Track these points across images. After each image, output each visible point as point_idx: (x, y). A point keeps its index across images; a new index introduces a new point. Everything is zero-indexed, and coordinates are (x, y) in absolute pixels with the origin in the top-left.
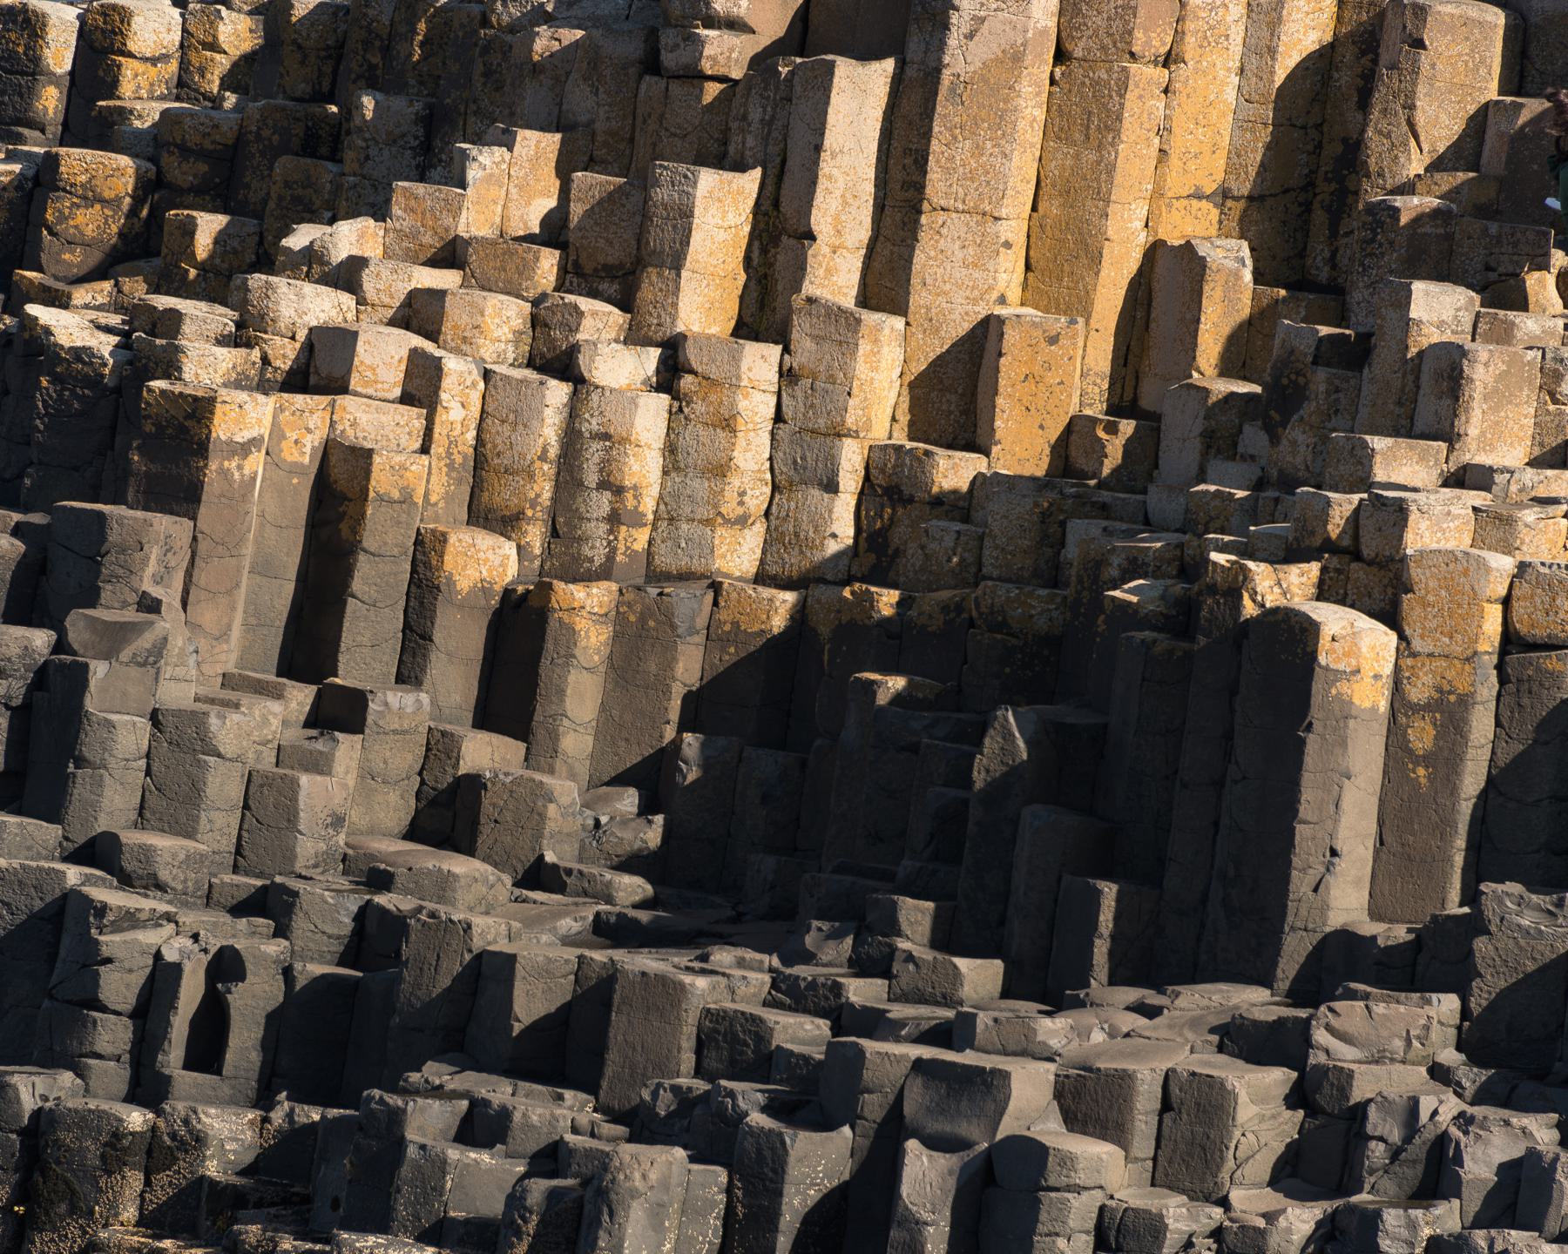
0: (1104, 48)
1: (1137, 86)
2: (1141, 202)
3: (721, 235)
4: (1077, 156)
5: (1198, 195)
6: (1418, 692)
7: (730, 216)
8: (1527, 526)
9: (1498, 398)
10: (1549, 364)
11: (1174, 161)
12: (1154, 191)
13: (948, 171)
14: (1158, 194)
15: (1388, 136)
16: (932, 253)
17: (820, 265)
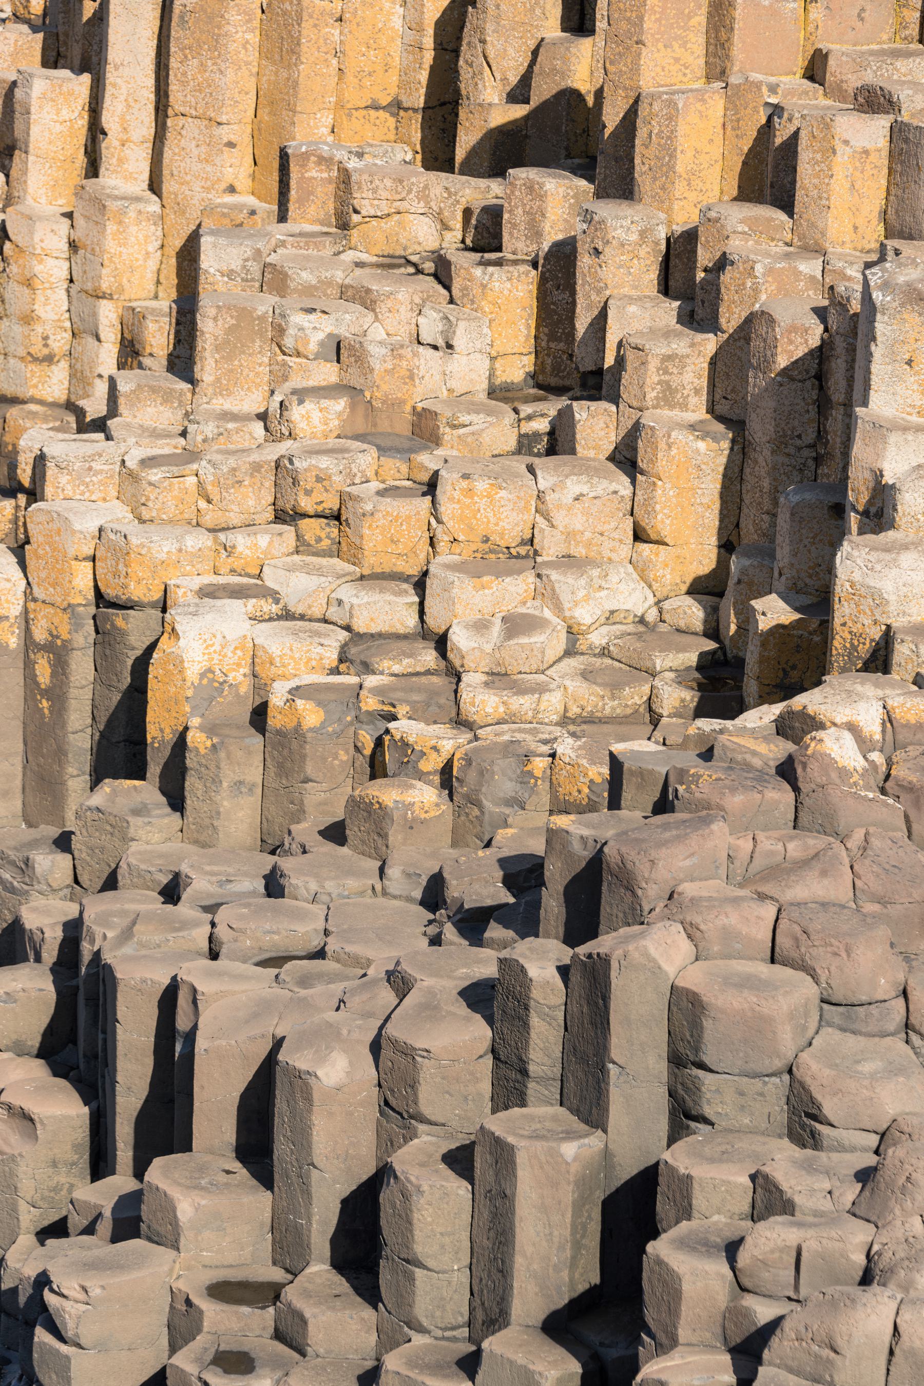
1: (311, 17)
2: (326, 113)
3: (58, 128)
4: (276, 74)
5: (377, 108)
6: (40, 635)
7: (64, 112)
8: (150, 484)
10: (279, 320)
11: (349, 77)
12: (336, 103)
13: (184, 84)
14: (340, 105)
15: (471, 66)
16: (177, 150)
17: (113, 155)
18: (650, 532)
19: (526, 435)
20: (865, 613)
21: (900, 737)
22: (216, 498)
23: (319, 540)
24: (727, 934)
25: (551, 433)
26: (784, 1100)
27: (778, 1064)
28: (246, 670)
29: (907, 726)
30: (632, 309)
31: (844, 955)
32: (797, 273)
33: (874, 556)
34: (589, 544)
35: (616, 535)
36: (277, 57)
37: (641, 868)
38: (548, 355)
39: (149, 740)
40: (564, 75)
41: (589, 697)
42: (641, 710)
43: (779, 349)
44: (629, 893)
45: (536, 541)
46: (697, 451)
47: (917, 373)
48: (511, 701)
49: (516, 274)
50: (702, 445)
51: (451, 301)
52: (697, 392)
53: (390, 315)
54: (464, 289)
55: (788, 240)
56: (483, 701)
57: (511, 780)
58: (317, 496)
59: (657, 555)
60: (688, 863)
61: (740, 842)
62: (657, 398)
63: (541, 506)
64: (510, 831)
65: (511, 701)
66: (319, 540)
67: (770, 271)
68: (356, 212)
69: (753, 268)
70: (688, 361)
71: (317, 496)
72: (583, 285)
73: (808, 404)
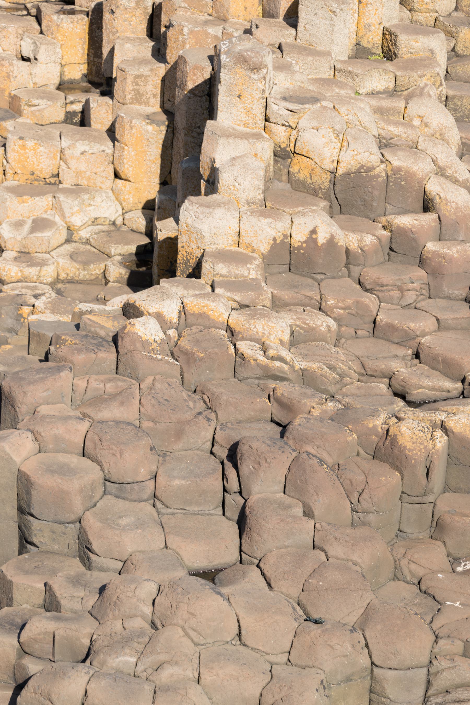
18: (121, 174)
19: (69, 112)
20: (193, 242)
21: (189, 321)
24: (57, 439)
25: (83, 112)
26: (76, 537)
27: (73, 517)
29: (193, 314)
30: (128, 46)
31: (118, 455)
32: (207, 34)
33: (200, 210)
34: (89, 179)
35: (104, 174)
37: (18, 396)
38: (94, 65)
41: (70, 269)
42: (100, 277)
43: (189, 78)
44: (13, 409)
45: (60, 175)
46: (147, 131)
47: (244, 103)
48: (25, 270)
49: (76, 20)
50: (150, 128)
51: (41, 33)
52: (154, 96)
53: (5, 39)
54: (48, 26)
55: (210, 13)
56: (9, 269)
57: (11, 318)
59: (125, 187)
60: (45, 394)
61: (80, 382)
62: (132, 98)
63: (63, 157)
64: (8, 347)
65: (25, 270)
67: (191, 32)
69: (182, 30)
70: (149, 79)
72: (106, 29)
73: (204, 110)
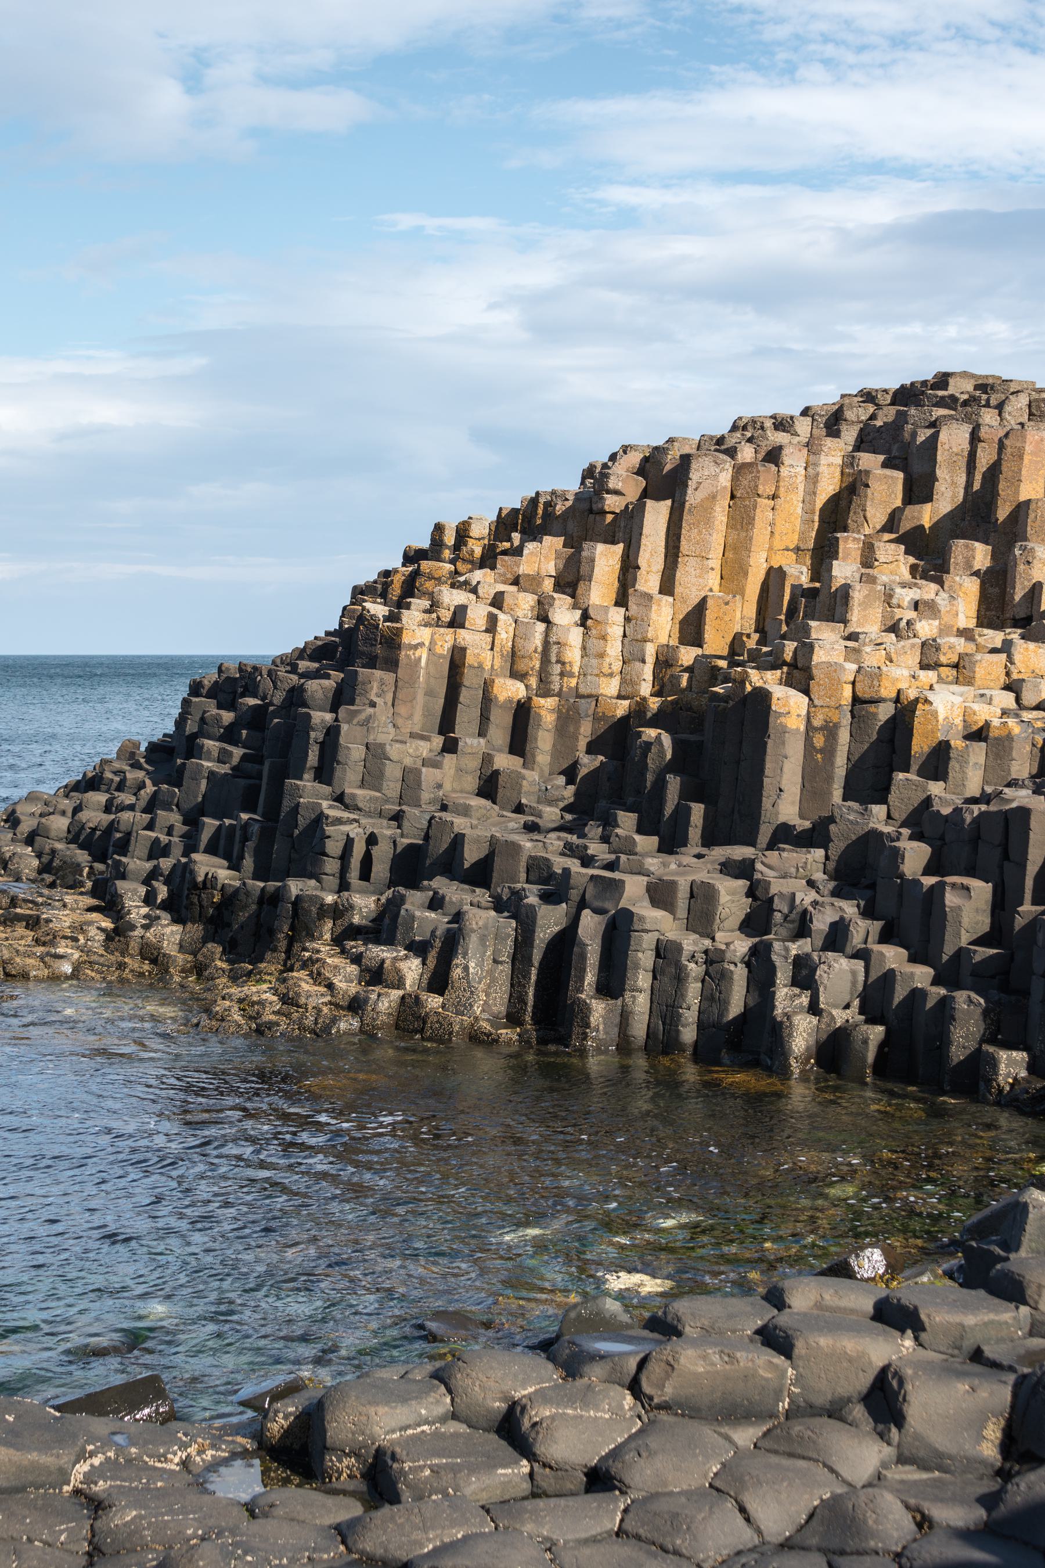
0: (748, 493)
3: (607, 569)
5: (788, 550)
6: (817, 723)
9: (865, 605)
10: (888, 591)
11: (777, 535)
13: (689, 541)
14: (771, 549)
22: (895, 660)
23: (948, 677)
28: (961, 718)
36: (739, 527)
39: (913, 753)
40: (919, 519)
58: (948, 656)
66: (948, 677)
68: (876, 560)
71: (948, 656)
